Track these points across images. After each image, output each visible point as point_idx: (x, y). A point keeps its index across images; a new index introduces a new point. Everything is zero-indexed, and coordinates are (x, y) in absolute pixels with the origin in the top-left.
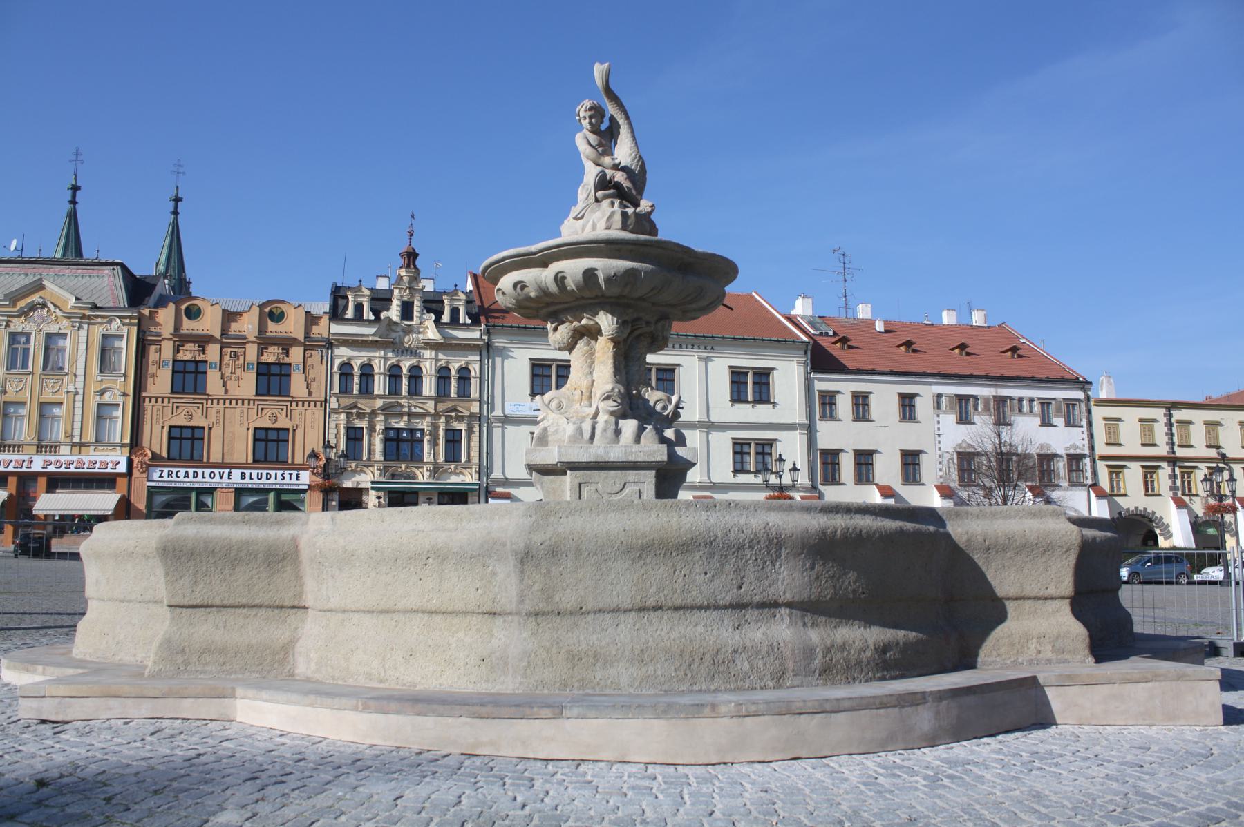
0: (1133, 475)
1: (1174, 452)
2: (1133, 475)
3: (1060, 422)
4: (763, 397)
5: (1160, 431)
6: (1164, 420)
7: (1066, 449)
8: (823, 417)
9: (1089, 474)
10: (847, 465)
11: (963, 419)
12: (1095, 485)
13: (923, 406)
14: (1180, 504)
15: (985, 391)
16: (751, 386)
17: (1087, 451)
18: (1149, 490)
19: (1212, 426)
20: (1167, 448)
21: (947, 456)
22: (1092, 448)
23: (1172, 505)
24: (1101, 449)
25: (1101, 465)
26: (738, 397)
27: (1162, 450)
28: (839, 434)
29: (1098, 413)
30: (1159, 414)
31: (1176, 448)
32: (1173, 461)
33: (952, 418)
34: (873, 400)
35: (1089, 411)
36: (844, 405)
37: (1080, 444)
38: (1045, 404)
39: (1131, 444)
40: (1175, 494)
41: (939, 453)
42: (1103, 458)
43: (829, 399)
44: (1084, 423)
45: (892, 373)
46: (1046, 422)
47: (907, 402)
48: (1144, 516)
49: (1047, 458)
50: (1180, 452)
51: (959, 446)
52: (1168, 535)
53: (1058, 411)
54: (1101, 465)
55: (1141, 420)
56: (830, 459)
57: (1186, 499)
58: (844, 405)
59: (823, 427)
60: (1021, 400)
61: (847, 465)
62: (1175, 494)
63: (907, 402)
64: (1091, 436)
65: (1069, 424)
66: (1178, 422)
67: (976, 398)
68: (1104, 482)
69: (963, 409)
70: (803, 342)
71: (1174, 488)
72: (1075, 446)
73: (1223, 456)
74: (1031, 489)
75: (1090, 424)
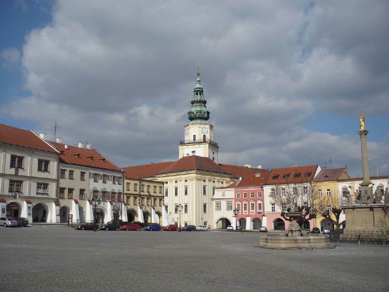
0: (132, 199)
1: (140, 193)
2: (132, 199)
3: (117, 183)
4: (46, 170)
5: (138, 187)
6: (139, 184)
7: (118, 191)
8: (61, 178)
9: (122, 198)
10: (66, 192)
11: (95, 181)
12: (123, 202)
13: (86, 176)
14: (141, 208)
15: (101, 173)
16: (43, 166)
17: (122, 192)
18: (135, 205)
19: (148, 186)
20: (139, 192)
21: (91, 191)
22: (123, 191)
23: (139, 207)
24: (126, 192)
25: (125, 195)
26: (40, 169)
27: (138, 193)
28: (65, 183)
29: (126, 181)
30: (138, 182)
31: (141, 192)
32: (140, 195)
33: (92, 180)
34: (74, 173)
35: (124, 180)
36: (67, 174)
37: (121, 190)
38: (114, 177)
39: (132, 191)
40: (140, 205)
41: (89, 190)
42: (126, 194)
43: (63, 171)
44: (122, 184)
45: (79, 165)
46: (114, 183)
47: (83, 174)
48: (132, 210)
49: (114, 193)
50: (142, 193)
51: (94, 188)
52: (137, 216)
53: (117, 180)
54: (125, 195)
55: (134, 184)
56: (62, 190)
57: (142, 206)
58: (67, 174)
59: (61, 181)
60: (109, 176)
61: (66, 192)
62: (140, 205)
63: (83, 174)
64: (123, 188)
65: (119, 184)
66: (142, 185)
67: (99, 174)
68: (125, 201)
69: (96, 177)
70: (59, 153)
71: (139, 203)
72: (120, 190)
73: (150, 195)
74: (110, 202)
75: (123, 184)
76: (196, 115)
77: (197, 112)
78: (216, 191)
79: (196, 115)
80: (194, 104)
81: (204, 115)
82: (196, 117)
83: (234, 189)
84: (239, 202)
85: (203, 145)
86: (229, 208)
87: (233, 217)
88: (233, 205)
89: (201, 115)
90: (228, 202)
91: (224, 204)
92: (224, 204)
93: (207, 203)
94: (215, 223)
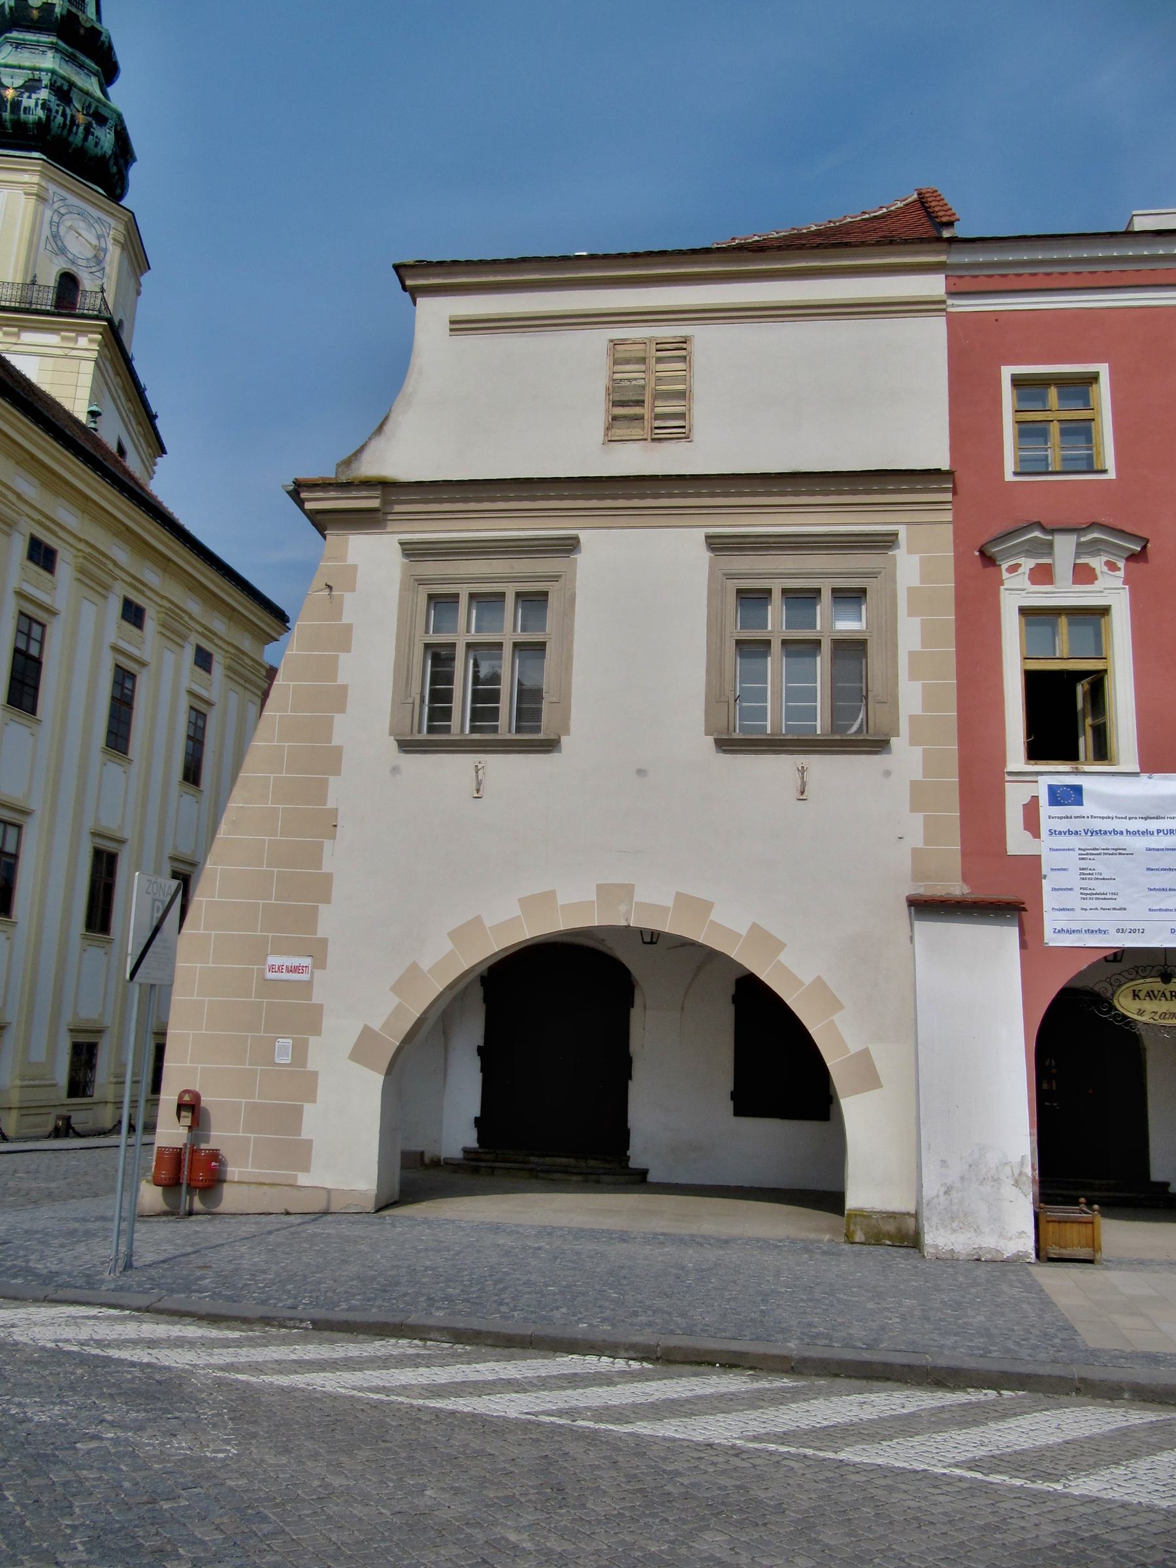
76: (16, 105)
77: (31, 86)
78: (459, 326)
79: (16, 105)
80: (15, 34)
81: (88, 131)
82: (19, 125)
83: (933, 285)
84: (1083, 575)
85: (53, 339)
86: (794, 681)
87: (925, 907)
88: (910, 634)
89: (64, 115)
90: (779, 571)
91: (640, 609)
92: (640, 609)
93: (36, 804)
94: (361, 1053)
